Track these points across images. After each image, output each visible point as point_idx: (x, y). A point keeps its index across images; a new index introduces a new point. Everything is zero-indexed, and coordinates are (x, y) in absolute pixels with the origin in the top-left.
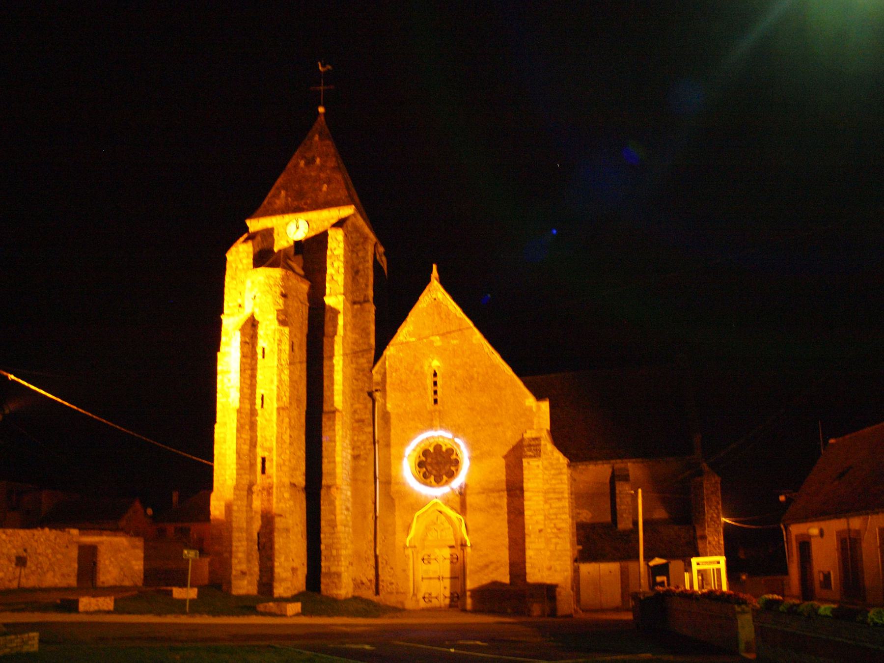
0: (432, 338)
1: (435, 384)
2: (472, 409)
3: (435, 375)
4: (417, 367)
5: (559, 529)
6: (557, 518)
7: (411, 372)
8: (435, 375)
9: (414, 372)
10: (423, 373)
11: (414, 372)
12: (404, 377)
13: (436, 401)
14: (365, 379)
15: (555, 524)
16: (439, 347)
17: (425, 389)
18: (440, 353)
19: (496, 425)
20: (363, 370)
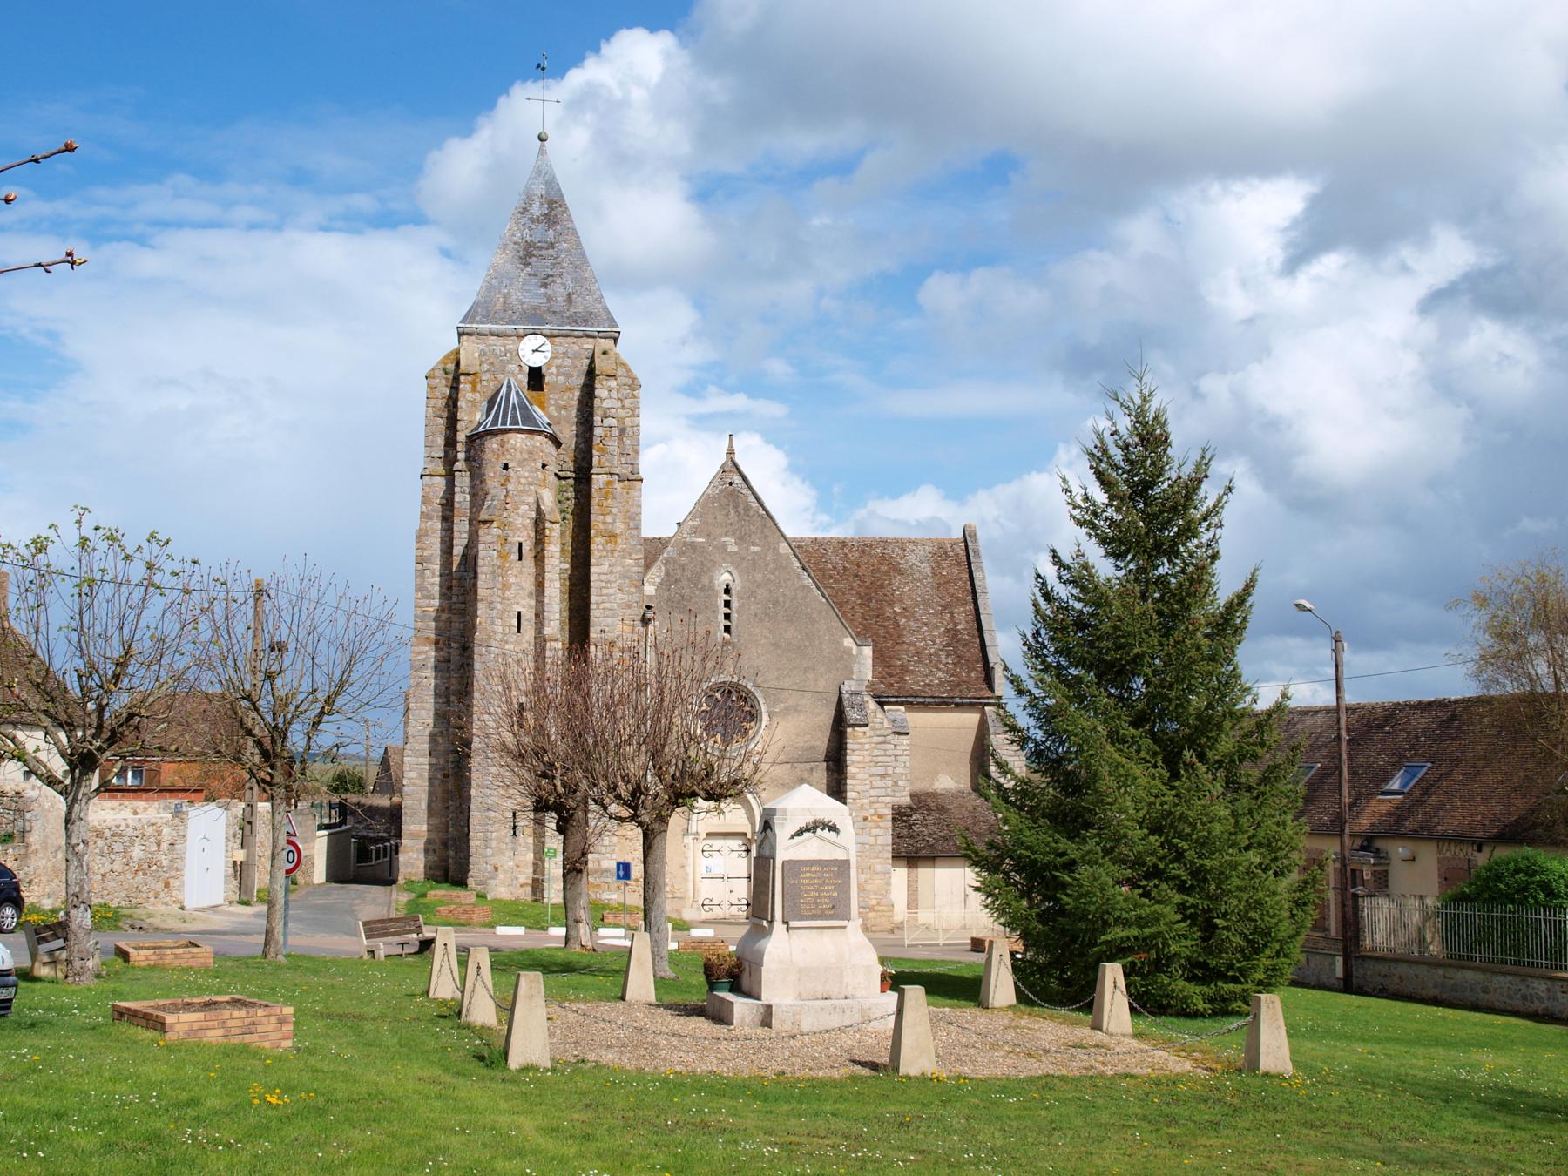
0: (726, 539)
1: (727, 604)
2: (776, 646)
3: (727, 591)
4: (705, 580)
5: (880, 817)
6: (878, 802)
7: (696, 585)
8: (727, 591)
9: (700, 586)
10: (712, 588)
11: (700, 586)
12: (686, 592)
13: (727, 629)
14: (633, 590)
15: (875, 809)
16: (736, 553)
17: (715, 611)
18: (737, 560)
19: (806, 670)
20: (630, 578)
